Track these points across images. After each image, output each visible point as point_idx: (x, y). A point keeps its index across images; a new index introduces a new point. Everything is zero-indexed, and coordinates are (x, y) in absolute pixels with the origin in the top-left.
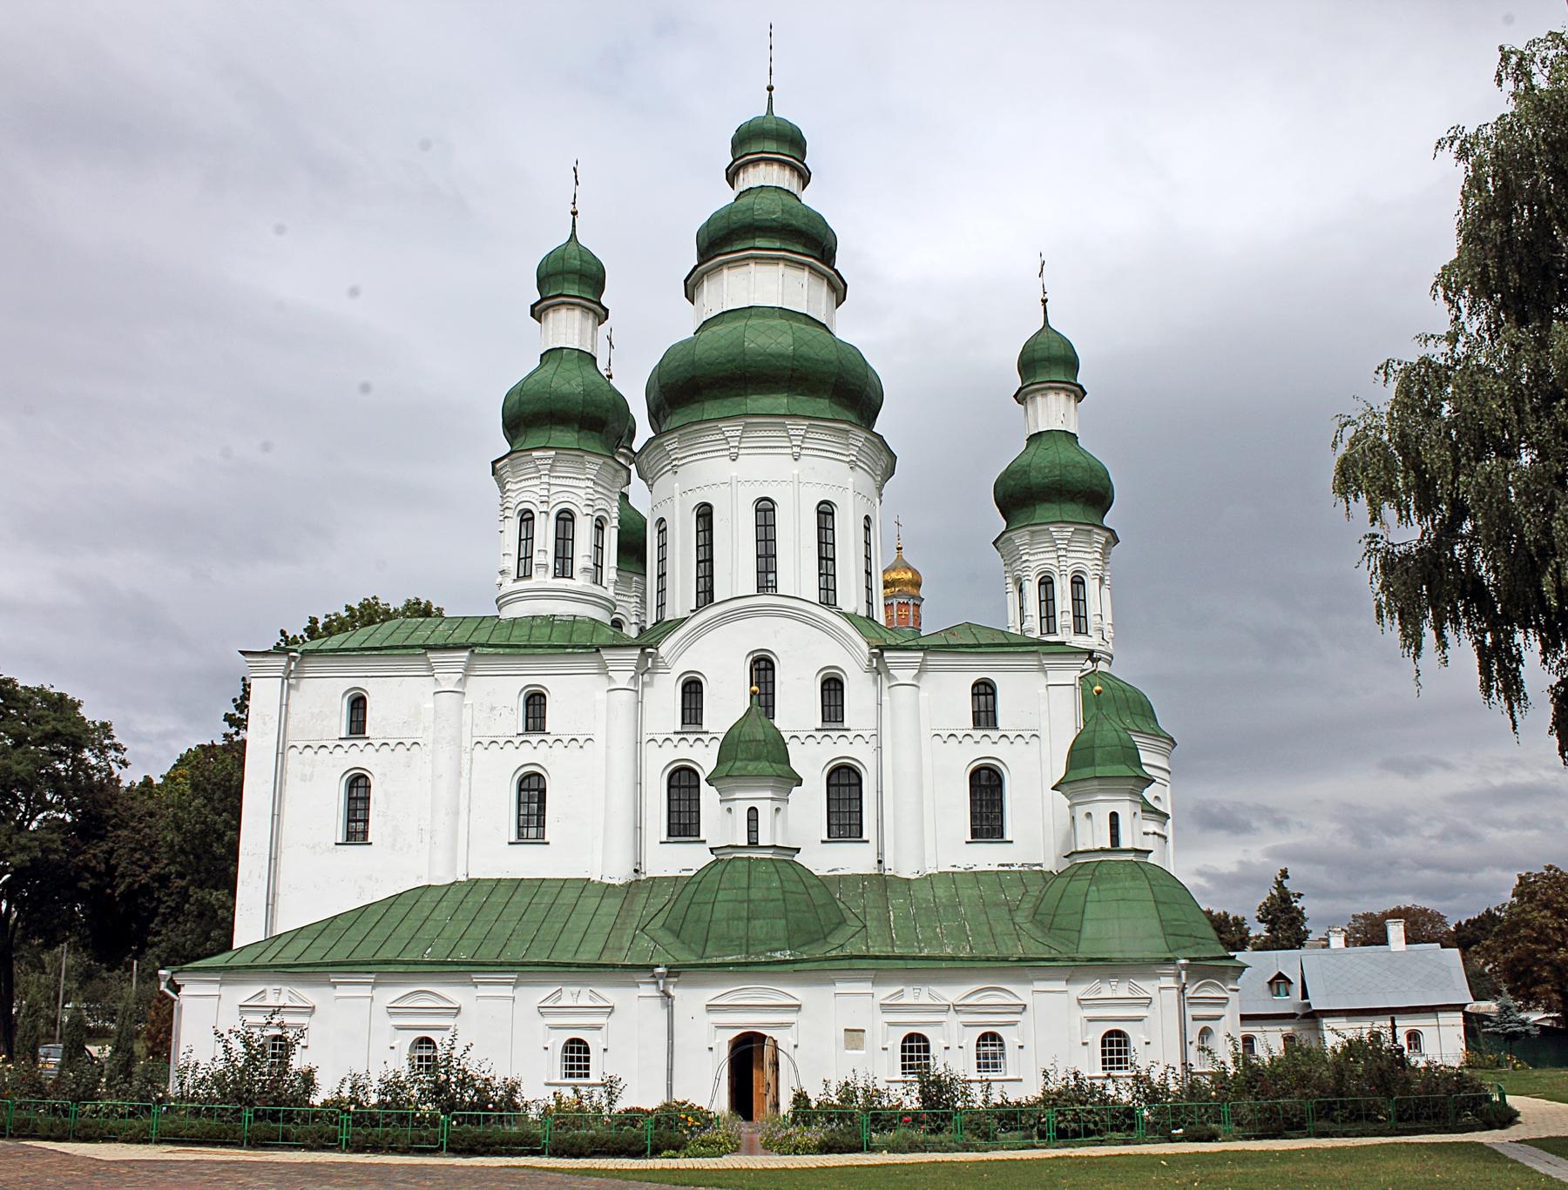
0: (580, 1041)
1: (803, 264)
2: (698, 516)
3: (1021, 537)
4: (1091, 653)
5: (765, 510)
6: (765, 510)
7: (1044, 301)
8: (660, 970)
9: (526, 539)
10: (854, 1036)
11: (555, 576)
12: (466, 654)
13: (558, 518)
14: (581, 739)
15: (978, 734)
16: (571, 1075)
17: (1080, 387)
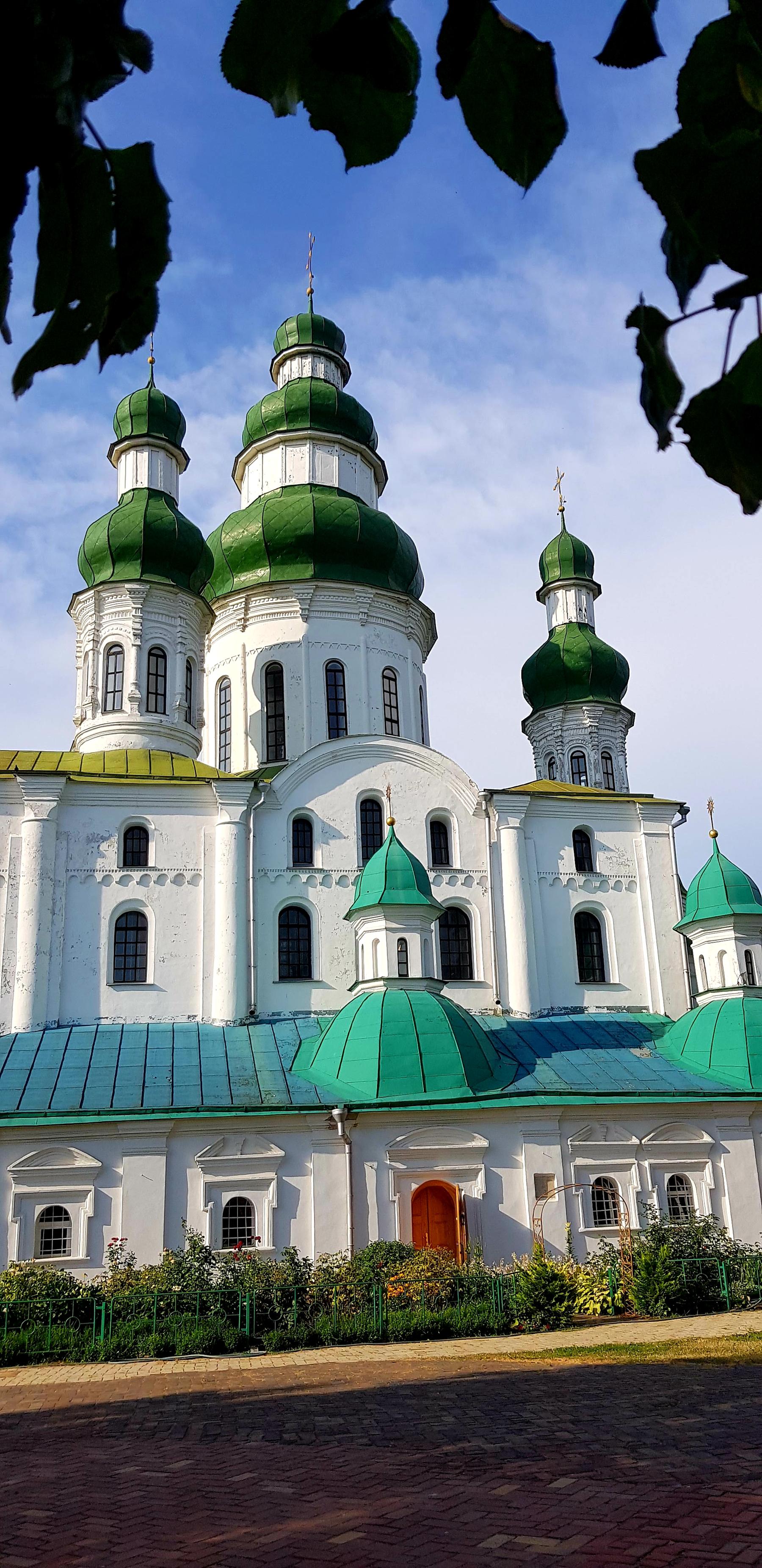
0: (243, 1201)
1: (355, 450)
2: (267, 674)
3: (555, 714)
4: (681, 805)
5: (334, 673)
6: (334, 673)
7: (562, 510)
8: (336, 1112)
9: (114, 673)
10: (541, 1185)
11: (147, 711)
12: (63, 780)
13: (150, 654)
14: (188, 875)
15: (580, 879)
16: (232, 1243)
17: (599, 586)
